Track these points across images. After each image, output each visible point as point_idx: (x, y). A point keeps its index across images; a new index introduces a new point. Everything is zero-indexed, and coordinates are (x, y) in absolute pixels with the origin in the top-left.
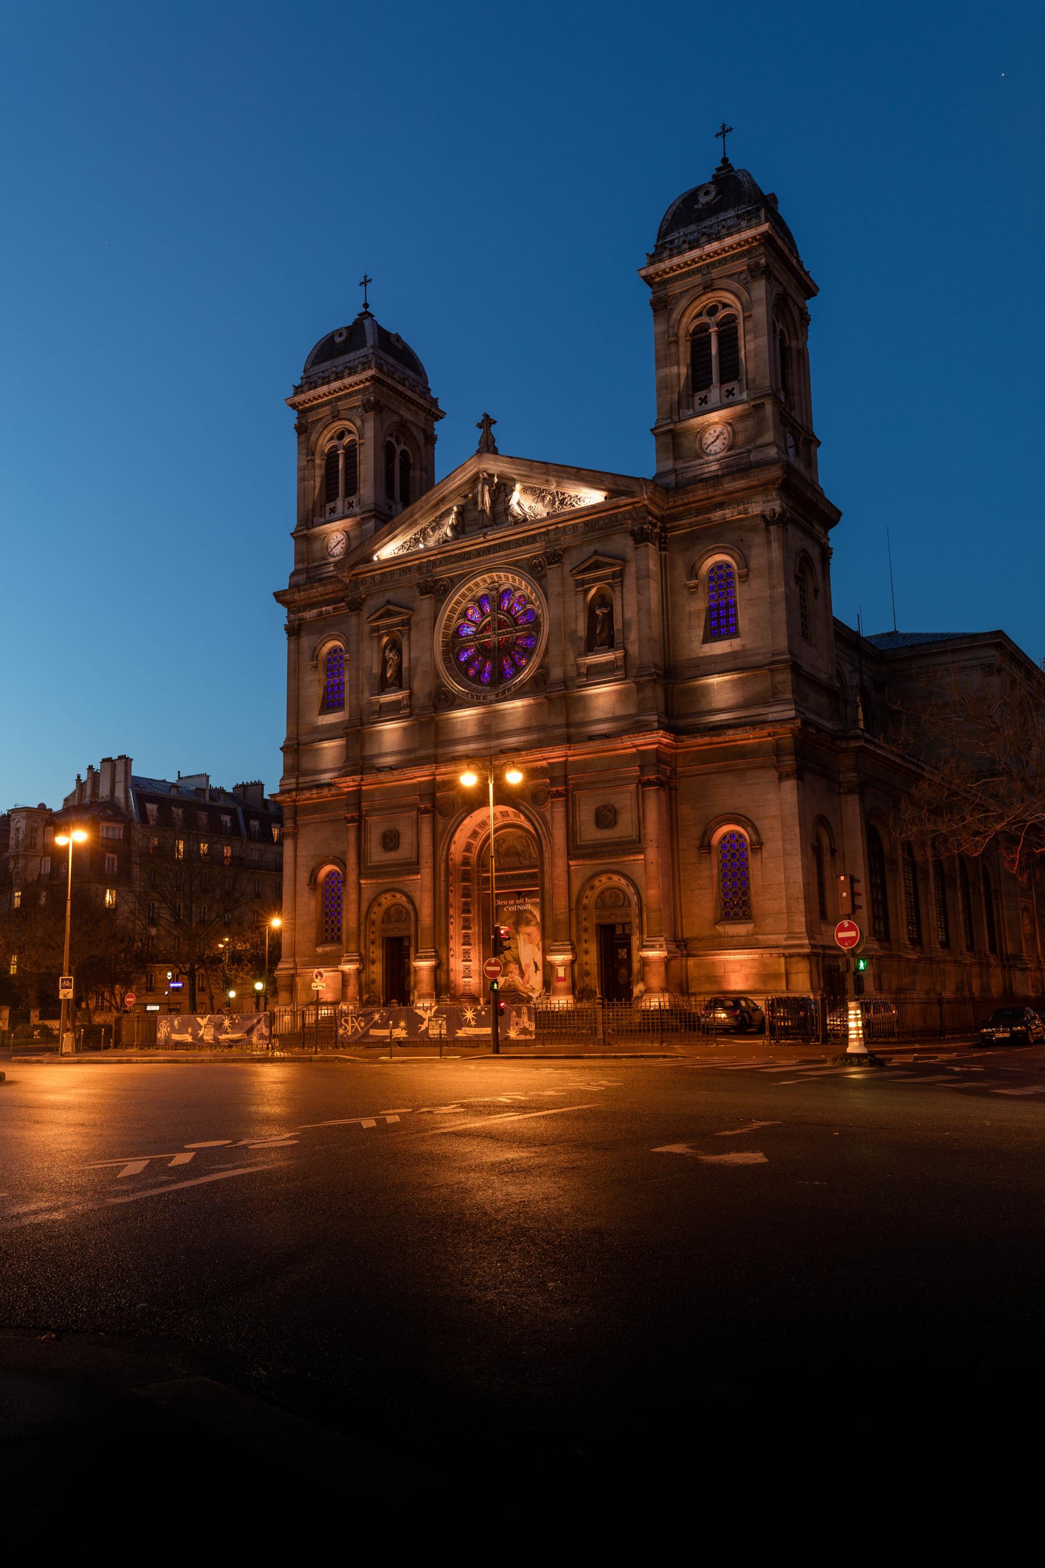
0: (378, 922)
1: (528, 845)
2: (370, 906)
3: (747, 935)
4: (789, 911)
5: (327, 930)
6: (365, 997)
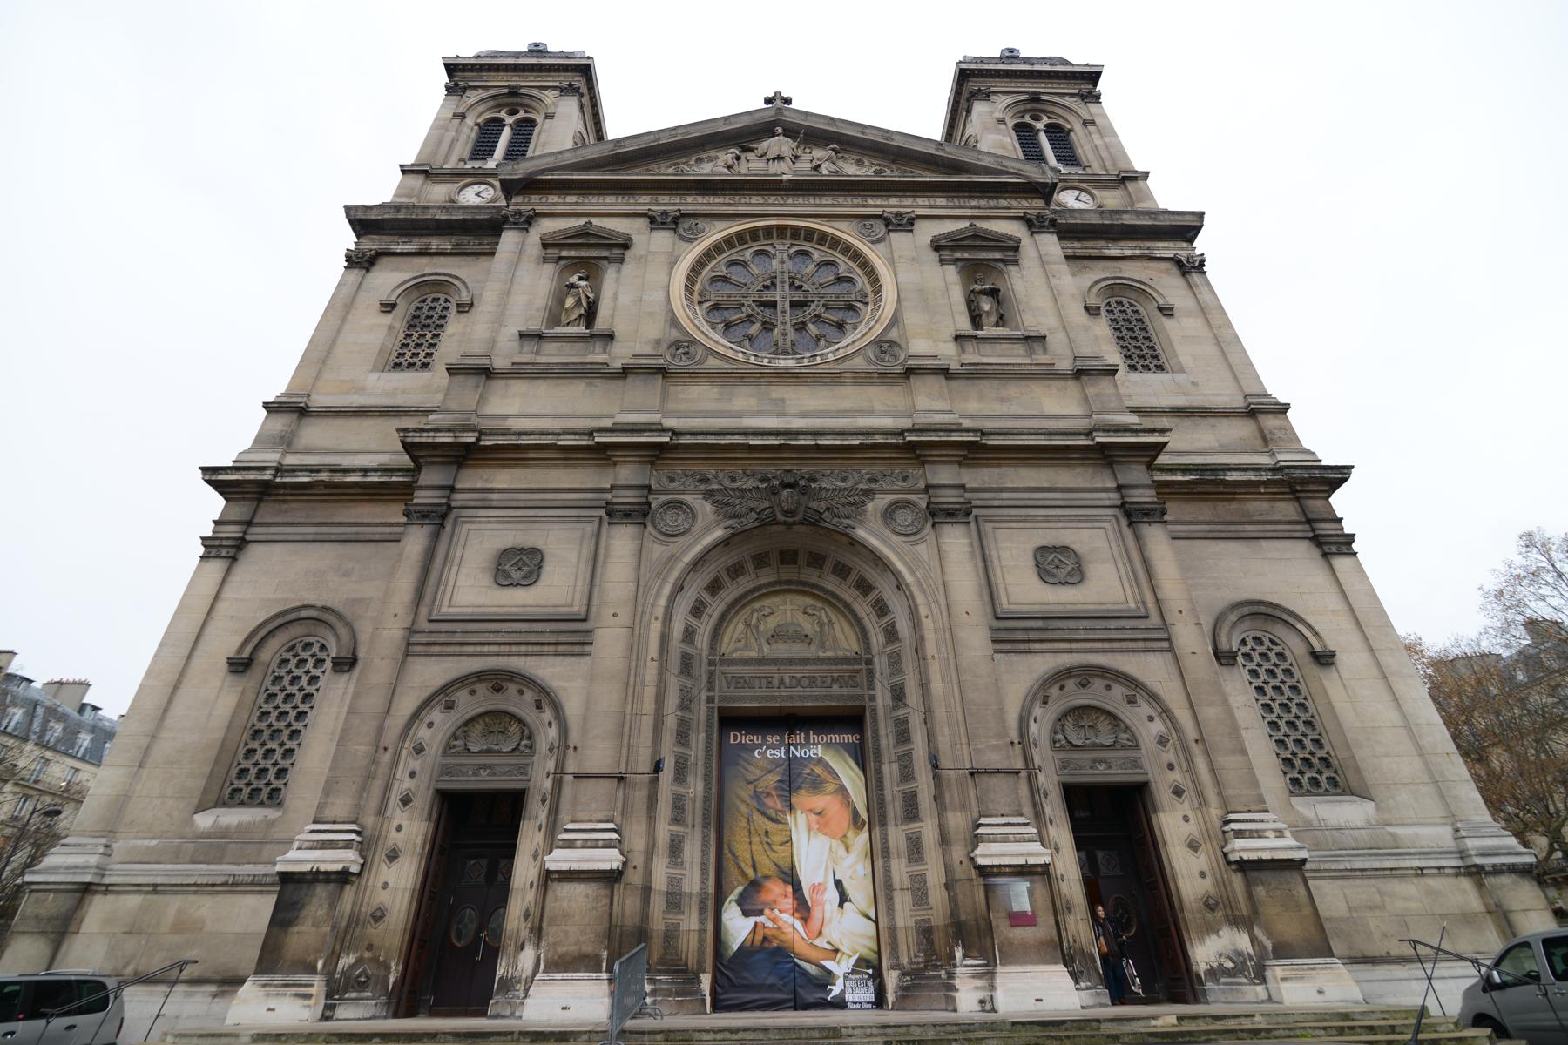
1: (831, 623)
2: (427, 704)
3: (1369, 826)
4: (1438, 783)
5: (243, 772)
6: (346, 961)
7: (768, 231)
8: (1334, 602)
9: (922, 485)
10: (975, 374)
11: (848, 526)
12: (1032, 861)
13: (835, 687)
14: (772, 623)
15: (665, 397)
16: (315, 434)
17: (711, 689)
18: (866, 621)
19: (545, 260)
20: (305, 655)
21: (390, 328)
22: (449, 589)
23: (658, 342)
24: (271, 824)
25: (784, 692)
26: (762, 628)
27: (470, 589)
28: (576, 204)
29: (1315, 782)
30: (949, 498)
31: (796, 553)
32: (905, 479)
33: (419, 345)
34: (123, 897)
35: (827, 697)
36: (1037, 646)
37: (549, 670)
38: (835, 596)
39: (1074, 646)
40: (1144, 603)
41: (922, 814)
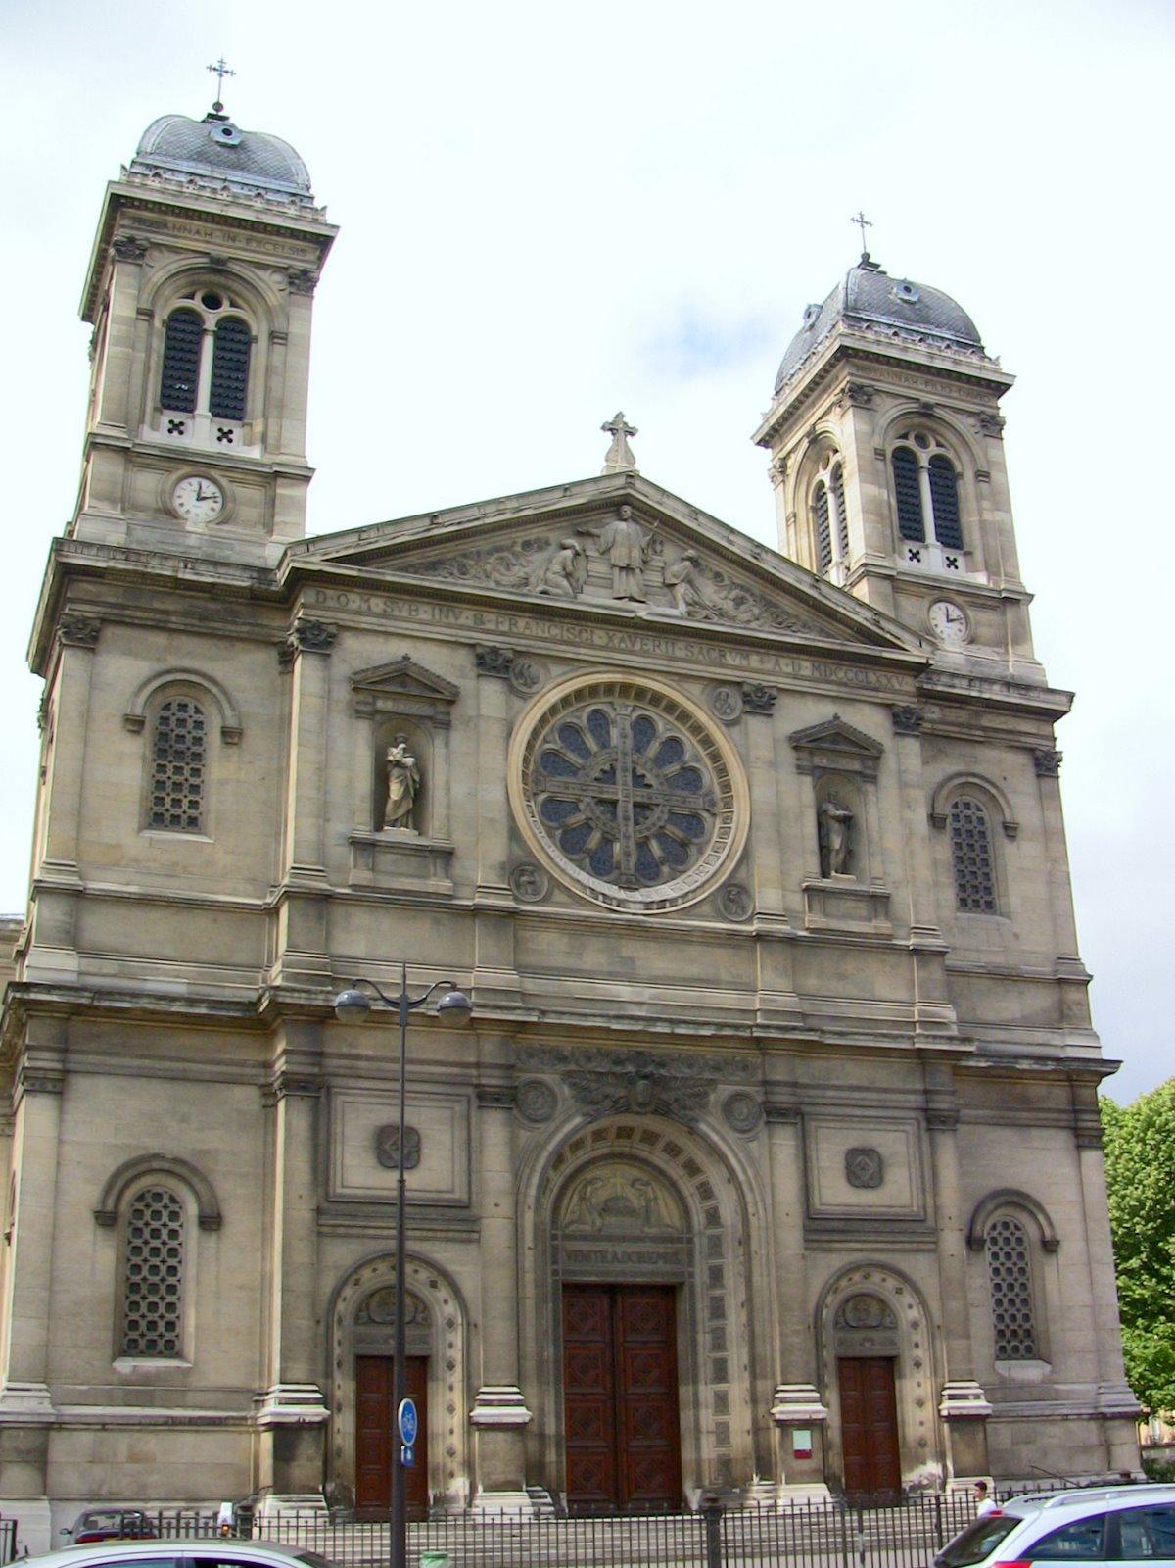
0: (348, 1321)
1: (656, 1198)
2: (343, 1283)
7: (610, 688)
8: (1072, 1193)
9: (760, 1077)
10: (821, 941)
11: (693, 1119)
12: (814, 1417)
13: (660, 1264)
14: (603, 1195)
15: (517, 945)
16: (101, 927)
17: (555, 1262)
18: (690, 1201)
19: (359, 714)
20: (157, 1206)
21: (144, 758)
22: (339, 1168)
23: (503, 866)
24: (187, 1372)
25: (619, 1267)
26: (594, 1200)
27: (360, 1173)
28: (384, 615)
29: (1016, 1349)
30: (782, 1097)
31: (632, 1129)
32: (745, 1068)
33: (177, 786)
34: (76, 1433)
35: (653, 1273)
36: (838, 1245)
37: (445, 1254)
38: (661, 1172)
39: (865, 1246)
40: (925, 1208)
41: (730, 1377)
